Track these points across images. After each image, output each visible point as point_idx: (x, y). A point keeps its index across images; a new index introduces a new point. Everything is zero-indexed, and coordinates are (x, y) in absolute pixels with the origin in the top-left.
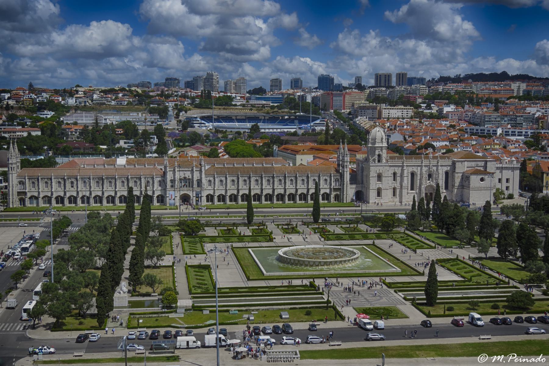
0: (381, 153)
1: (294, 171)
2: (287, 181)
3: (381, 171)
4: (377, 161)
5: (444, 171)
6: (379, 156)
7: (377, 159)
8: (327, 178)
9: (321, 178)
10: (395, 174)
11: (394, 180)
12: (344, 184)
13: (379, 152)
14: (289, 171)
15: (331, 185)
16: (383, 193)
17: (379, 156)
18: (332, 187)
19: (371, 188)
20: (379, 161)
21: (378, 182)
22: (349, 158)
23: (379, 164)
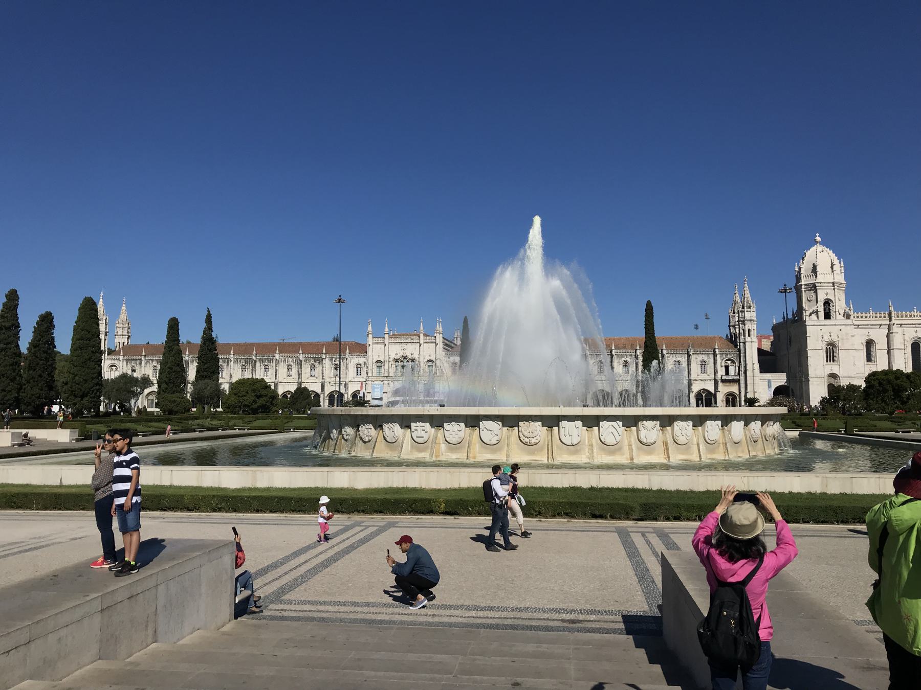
0: (833, 299)
2: (615, 364)
3: (834, 338)
4: (821, 314)
6: (827, 303)
8: (705, 358)
9: (693, 358)
10: (869, 344)
12: (745, 373)
13: (827, 294)
15: (716, 372)
17: (827, 303)
18: (719, 377)
19: (812, 372)
20: (827, 316)
22: (754, 314)
23: (828, 322)
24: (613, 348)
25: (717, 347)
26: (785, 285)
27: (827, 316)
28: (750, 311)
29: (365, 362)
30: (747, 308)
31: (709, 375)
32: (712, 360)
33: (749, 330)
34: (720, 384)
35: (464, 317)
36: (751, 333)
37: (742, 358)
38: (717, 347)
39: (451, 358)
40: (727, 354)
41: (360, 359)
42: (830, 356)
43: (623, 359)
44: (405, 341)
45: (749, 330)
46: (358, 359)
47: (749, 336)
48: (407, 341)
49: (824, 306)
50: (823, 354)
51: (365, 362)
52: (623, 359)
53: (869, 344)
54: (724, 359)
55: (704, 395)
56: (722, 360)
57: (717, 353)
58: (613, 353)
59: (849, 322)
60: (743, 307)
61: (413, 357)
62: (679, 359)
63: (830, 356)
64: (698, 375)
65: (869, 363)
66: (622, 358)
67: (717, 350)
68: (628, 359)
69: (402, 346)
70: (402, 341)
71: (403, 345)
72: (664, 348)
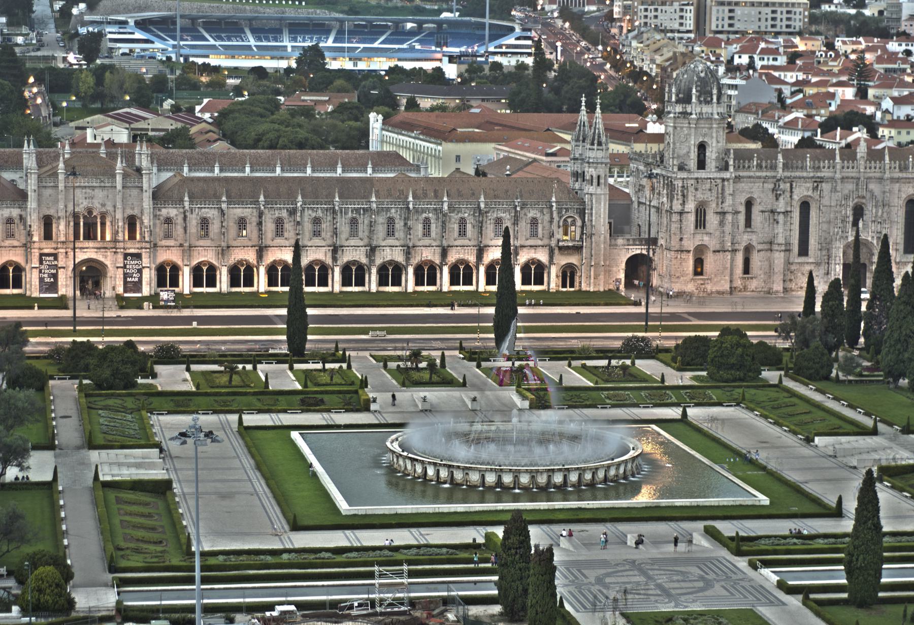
1: (436, 191)
3: (707, 196)
4: (692, 163)
5: (904, 196)
7: (694, 155)
10: (749, 204)
11: (748, 223)
14: (420, 192)
15: (552, 235)
16: (711, 262)
18: (553, 243)
20: (701, 165)
21: (699, 230)
23: (702, 174)
24: (411, 199)
25: (554, 199)
27: (701, 165)
28: (602, 150)
29: (21, 216)
31: (541, 240)
32: (547, 217)
33: (599, 177)
34: (556, 251)
36: (602, 181)
37: (586, 216)
38: (554, 199)
39: (163, 210)
40: (567, 209)
41: (12, 210)
42: (701, 220)
43: (424, 215)
44: (91, 184)
45: (599, 177)
46: (8, 210)
47: (598, 185)
48: (95, 184)
50: (692, 218)
51: (21, 216)
52: (424, 215)
53: (749, 204)
54: (563, 216)
56: (560, 218)
57: (554, 208)
58: (411, 206)
59: (726, 175)
60: (593, 144)
61: (104, 210)
62: (503, 215)
63: (701, 220)
65: (749, 230)
66: (422, 213)
67: (554, 204)
68: (430, 215)
69: (86, 193)
70: (86, 184)
71: (88, 190)
72: (482, 199)
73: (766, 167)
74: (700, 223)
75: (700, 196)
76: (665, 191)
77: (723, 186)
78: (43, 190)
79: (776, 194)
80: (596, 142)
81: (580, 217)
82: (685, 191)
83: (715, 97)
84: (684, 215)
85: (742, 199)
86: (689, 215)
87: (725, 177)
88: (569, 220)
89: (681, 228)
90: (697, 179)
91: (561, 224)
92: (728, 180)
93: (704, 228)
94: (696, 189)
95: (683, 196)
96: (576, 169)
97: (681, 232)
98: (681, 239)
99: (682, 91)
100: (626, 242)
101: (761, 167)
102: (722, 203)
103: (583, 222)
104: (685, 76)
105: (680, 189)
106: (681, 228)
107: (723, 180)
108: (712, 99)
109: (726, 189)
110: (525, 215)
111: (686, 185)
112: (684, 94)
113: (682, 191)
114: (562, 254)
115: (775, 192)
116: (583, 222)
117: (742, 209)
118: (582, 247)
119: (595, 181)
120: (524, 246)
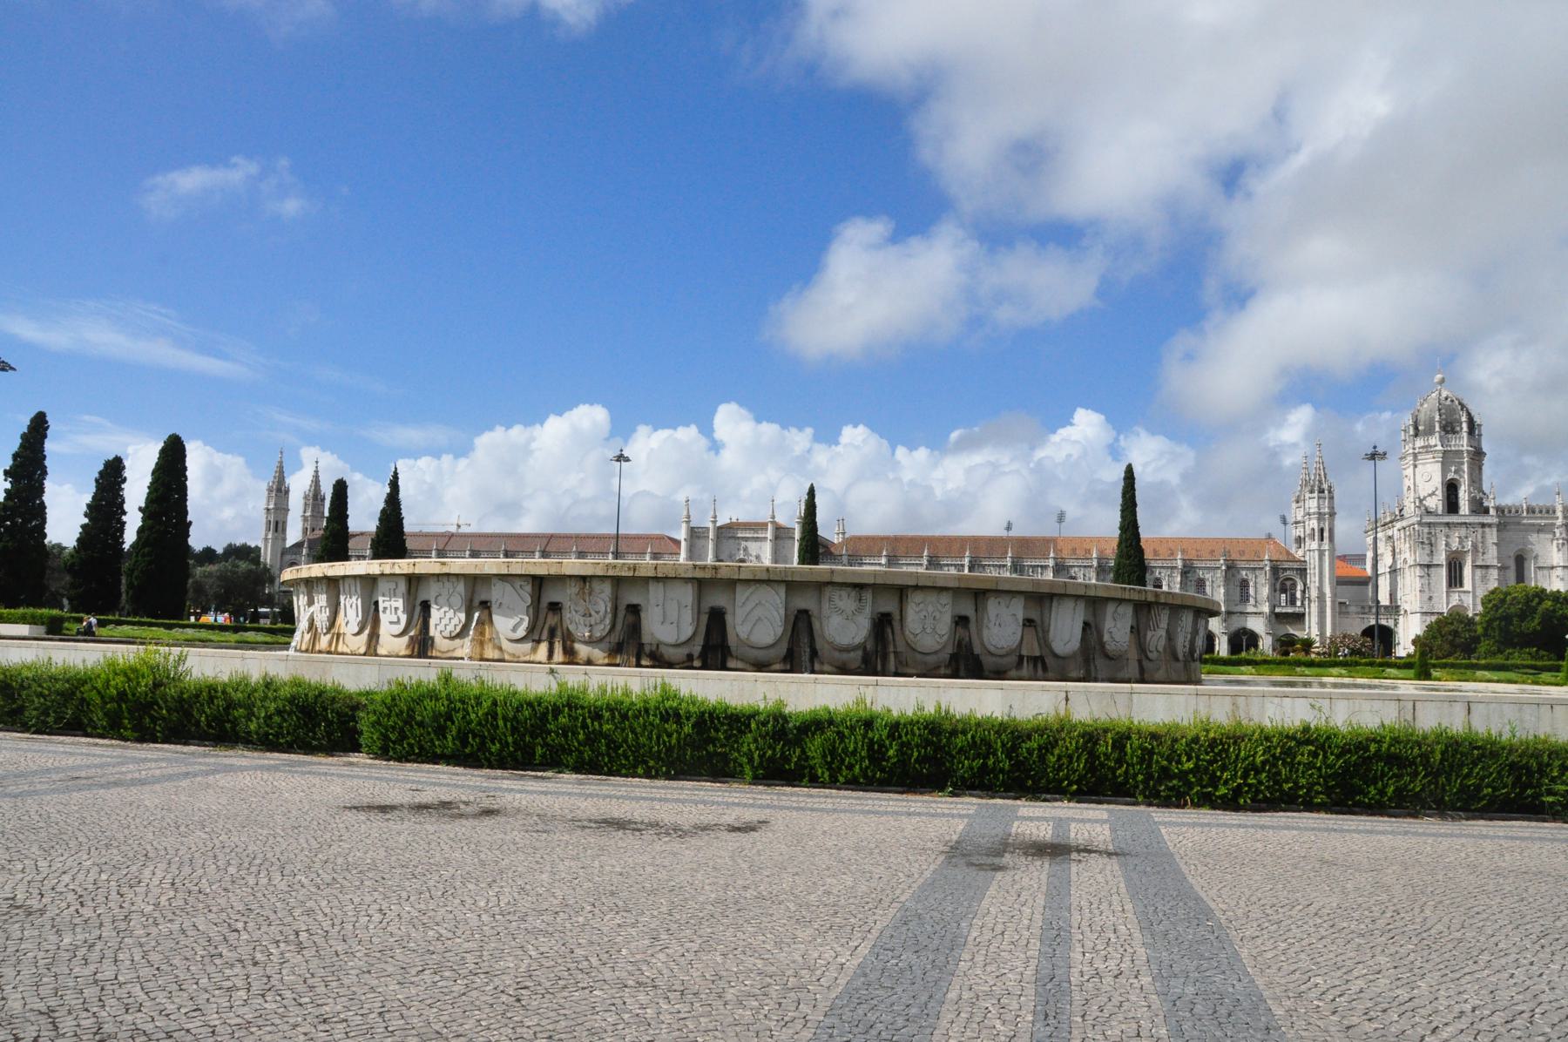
20: (1452, 506)
26: (1375, 447)
27: (1452, 506)
30: (1319, 492)
33: (1322, 531)
35: (808, 486)
36: (1326, 534)
45: (1322, 531)
48: (748, 535)
49: (1448, 490)
50: (1444, 572)
55: (1244, 638)
64: (1236, 605)
73: (1541, 512)
74: (1455, 579)
75: (1455, 545)
76: (1407, 545)
77: (1483, 532)
78: (697, 541)
79: (1558, 544)
80: (1316, 488)
81: (1301, 578)
82: (1433, 539)
83: (1465, 426)
84: (1432, 569)
85: (1512, 552)
86: (1439, 569)
87: (1485, 521)
88: (1288, 583)
89: (1429, 584)
90: (1448, 524)
91: (1278, 586)
92: (1490, 525)
93: (1461, 585)
94: (1447, 536)
95: (1431, 545)
96: (1298, 534)
97: (1430, 590)
98: (1430, 598)
99: (1422, 423)
100: (1359, 610)
101: (1534, 512)
102: (1484, 553)
103: (1305, 585)
104: (1426, 406)
105: (1426, 536)
106: (1429, 584)
107: (1483, 525)
108: (1462, 429)
109: (1488, 536)
110: (1233, 575)
111: (1433, 531)
112: (1425, 425)
113: (1428, 538)
114: (1281, 623)
115: (1555, 542)
116: (1305, 585)
117: (1512, 564)
118: (1304, 615)
119: (1316, 534)
120: (1234, 613)
